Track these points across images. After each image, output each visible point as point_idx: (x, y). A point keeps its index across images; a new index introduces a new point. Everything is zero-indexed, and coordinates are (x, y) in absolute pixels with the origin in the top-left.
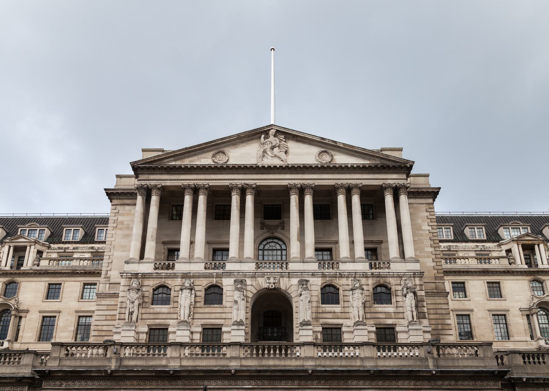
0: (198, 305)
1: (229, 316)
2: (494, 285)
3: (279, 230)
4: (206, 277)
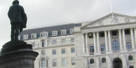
3: (117, 38)
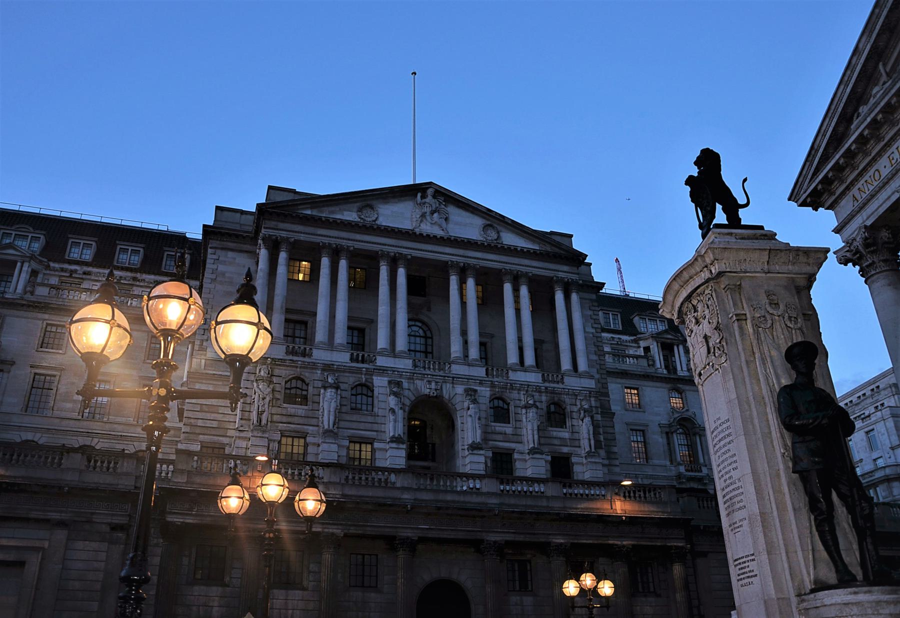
0: (344, 409)
1: (382, 428)
2: (633, 391)
4: (353, 373)
